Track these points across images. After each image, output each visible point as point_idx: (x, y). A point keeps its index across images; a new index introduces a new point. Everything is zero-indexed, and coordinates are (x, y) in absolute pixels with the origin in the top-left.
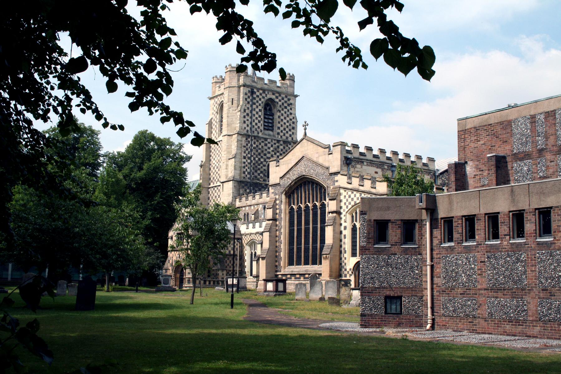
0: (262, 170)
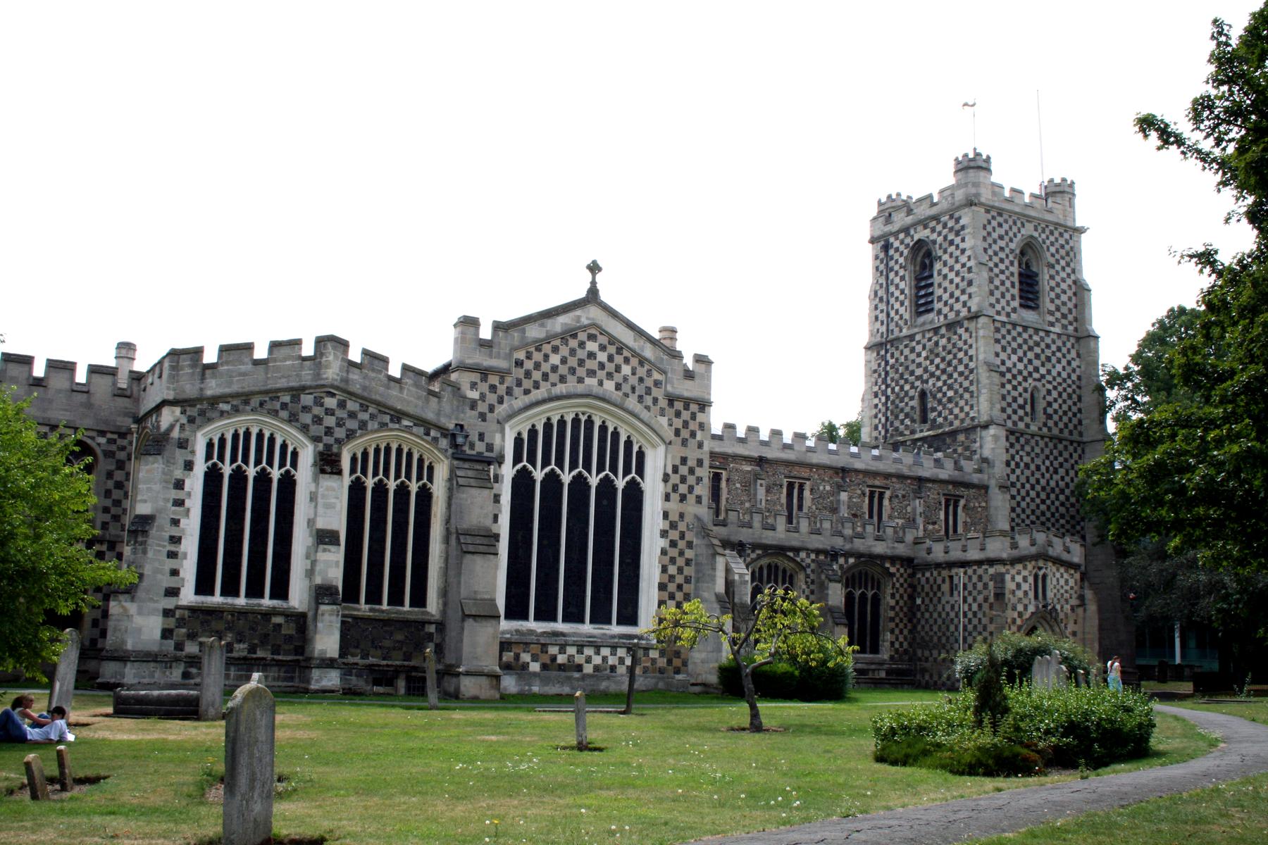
0: (907, 410)
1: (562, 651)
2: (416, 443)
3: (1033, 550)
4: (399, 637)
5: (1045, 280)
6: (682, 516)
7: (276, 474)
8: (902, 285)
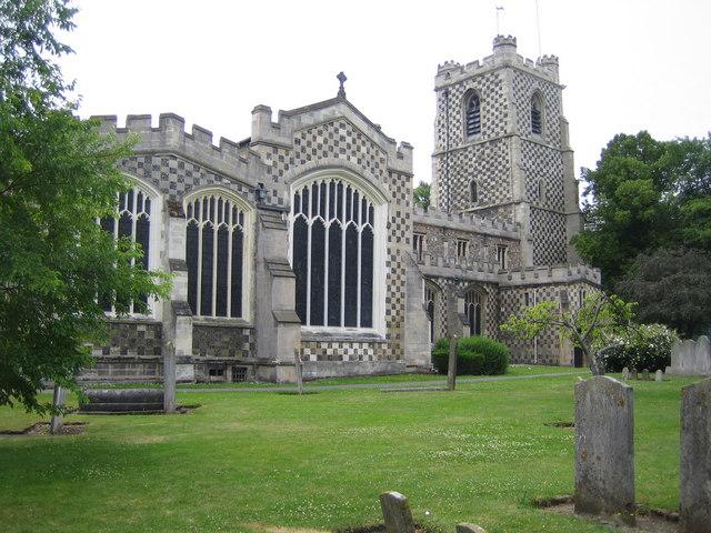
0: (463, 193)
1: (330, 346)
2: (232, 196)
3: (579, 276)
4: (226, 339)
5: (544, 117)
6: (398, 251)
7: (135, 217)
8: (458, 117)
